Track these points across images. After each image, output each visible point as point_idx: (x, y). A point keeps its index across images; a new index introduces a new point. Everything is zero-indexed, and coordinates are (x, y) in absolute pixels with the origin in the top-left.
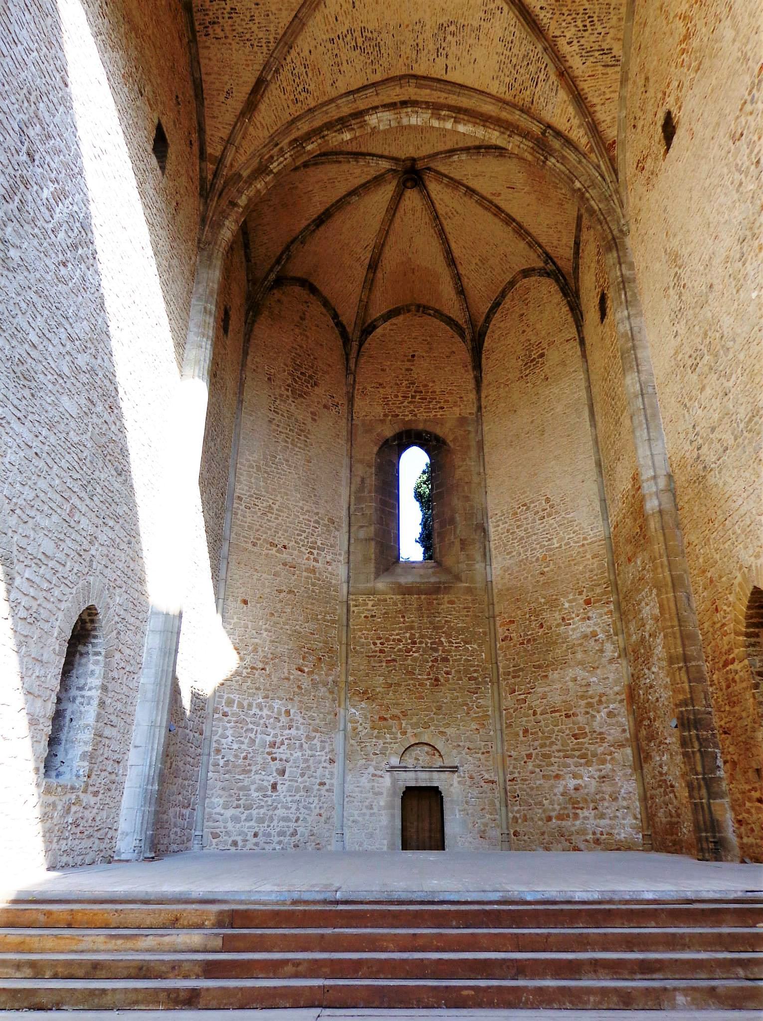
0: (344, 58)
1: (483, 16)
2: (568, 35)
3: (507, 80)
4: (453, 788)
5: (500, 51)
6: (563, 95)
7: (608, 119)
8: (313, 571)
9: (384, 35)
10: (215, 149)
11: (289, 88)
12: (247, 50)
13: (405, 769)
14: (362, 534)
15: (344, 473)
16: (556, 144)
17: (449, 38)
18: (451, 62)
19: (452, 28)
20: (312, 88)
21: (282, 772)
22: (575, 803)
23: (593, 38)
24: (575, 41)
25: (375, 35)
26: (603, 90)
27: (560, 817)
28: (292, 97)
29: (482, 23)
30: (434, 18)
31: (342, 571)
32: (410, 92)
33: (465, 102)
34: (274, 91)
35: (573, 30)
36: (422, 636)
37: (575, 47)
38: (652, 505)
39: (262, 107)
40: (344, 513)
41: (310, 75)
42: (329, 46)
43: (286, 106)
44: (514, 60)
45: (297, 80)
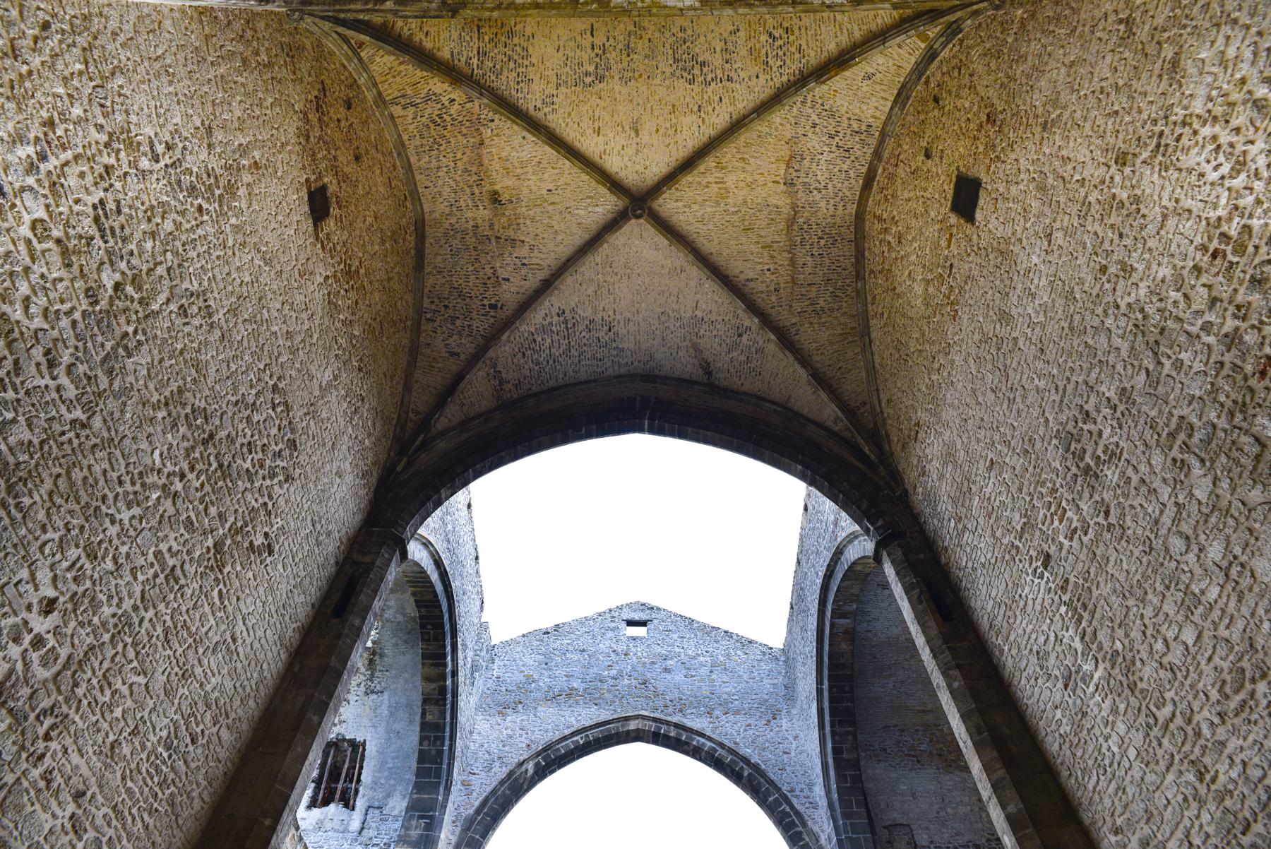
0: (718, 54)
1: (555, 99)
2: (456, 106)
3: (516, 40)
5: (530, 69)
6: (445, 54)
7: (378, 59)
9: (668, 70)
11: (793, 49)
12: (831, 102)
17: (591, 69)
18: (587, 41)
19: (588, 80)
20: (764, 38)
23: (429, 110)
24: (447, 103)
25: (678, 73)
26: (398, 79)
28: (791, 38)
29: (555, 92)
30: (611, 86)
34: (812, 54)
35: (452, 111)
37: (444, 100)
39: (832, 47)
41: (764, 51)
42: (733, 74)
43: (803, 30)
44: (512, 65)
45: (781, 53)
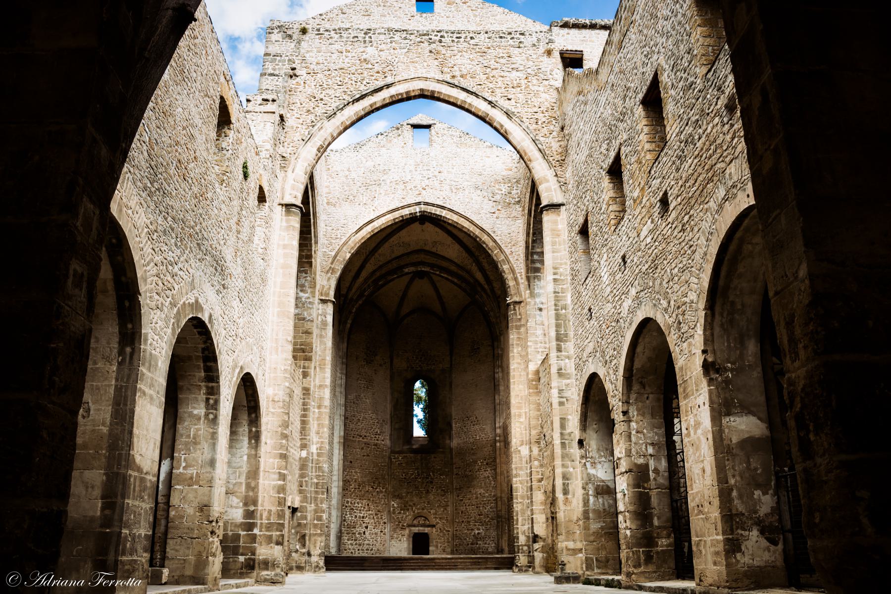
4: (433, 532)
8: (376, 445)
10: (344, 292)
13: (414, 526)
14: (397, 426)
15: (389, 398)
16: (479, 289)
21: (367, 527)
22: (477, 537)
27: (472, 544)
31: (388, 442)
32: (421, 257)
33: (445, 264)
36: (423, 472)
38: (498, 444)
40: (388, 417)
